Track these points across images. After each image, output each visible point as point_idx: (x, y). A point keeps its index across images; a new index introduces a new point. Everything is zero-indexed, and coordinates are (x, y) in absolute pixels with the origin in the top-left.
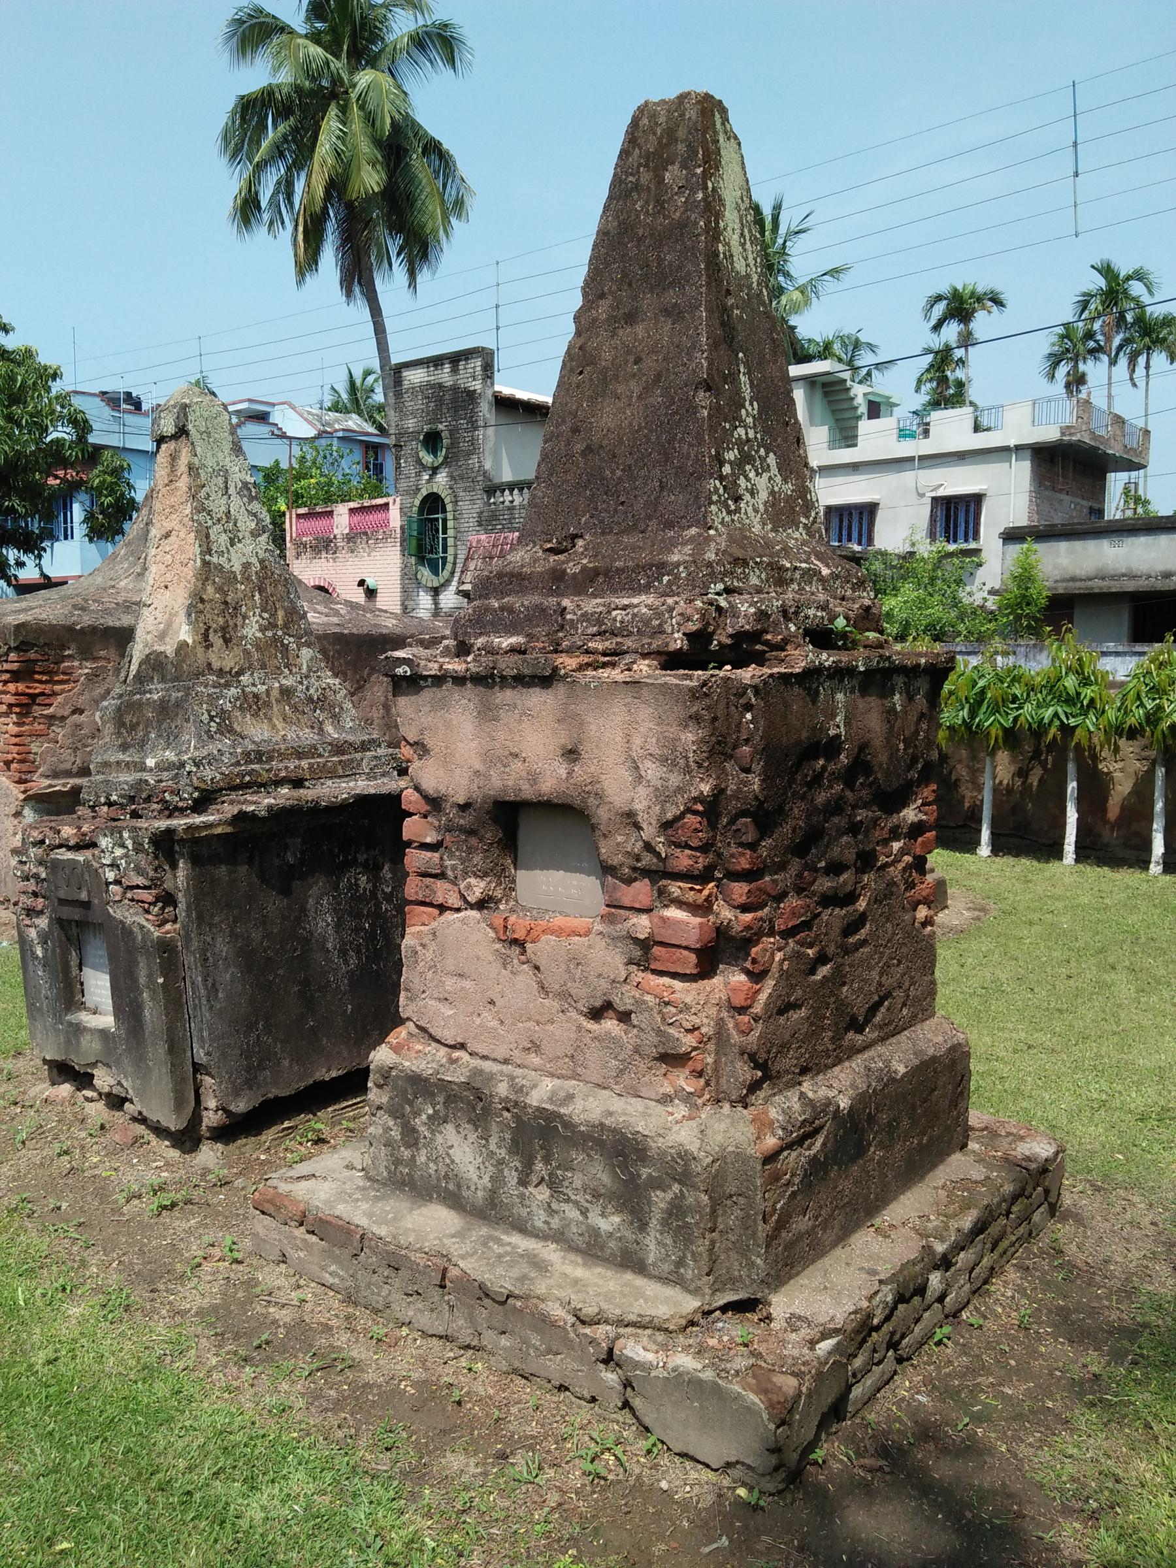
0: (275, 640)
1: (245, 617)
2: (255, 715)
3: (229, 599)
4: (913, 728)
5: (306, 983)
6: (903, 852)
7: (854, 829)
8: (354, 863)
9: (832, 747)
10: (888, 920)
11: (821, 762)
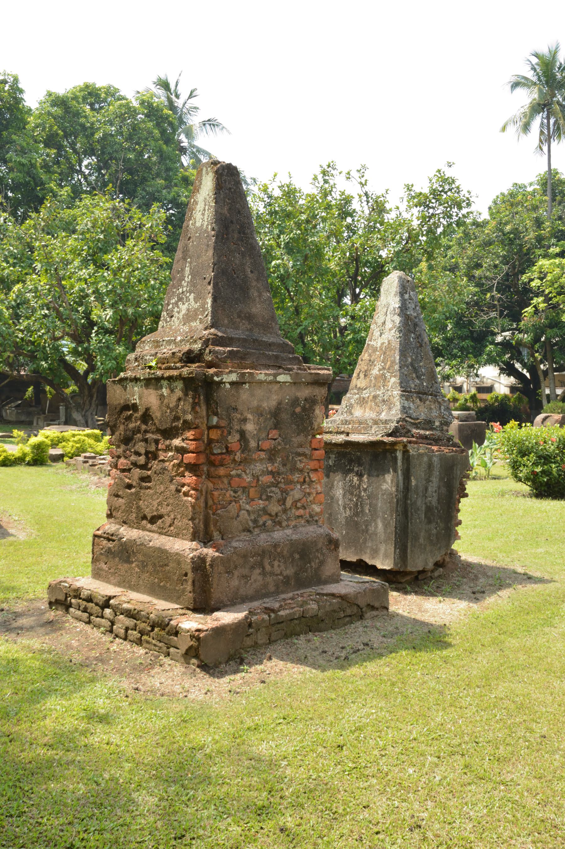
0: (383, 375)
1: (375, 366)
2: (361, 406)
3: (372, 359)
4: (174, 404)
5: (330, 515)
6: (173, 458)
7: (146, 441)
8: (350, 471)
9: (134, 407)
10: (161, 483)
11: (131, 412)
